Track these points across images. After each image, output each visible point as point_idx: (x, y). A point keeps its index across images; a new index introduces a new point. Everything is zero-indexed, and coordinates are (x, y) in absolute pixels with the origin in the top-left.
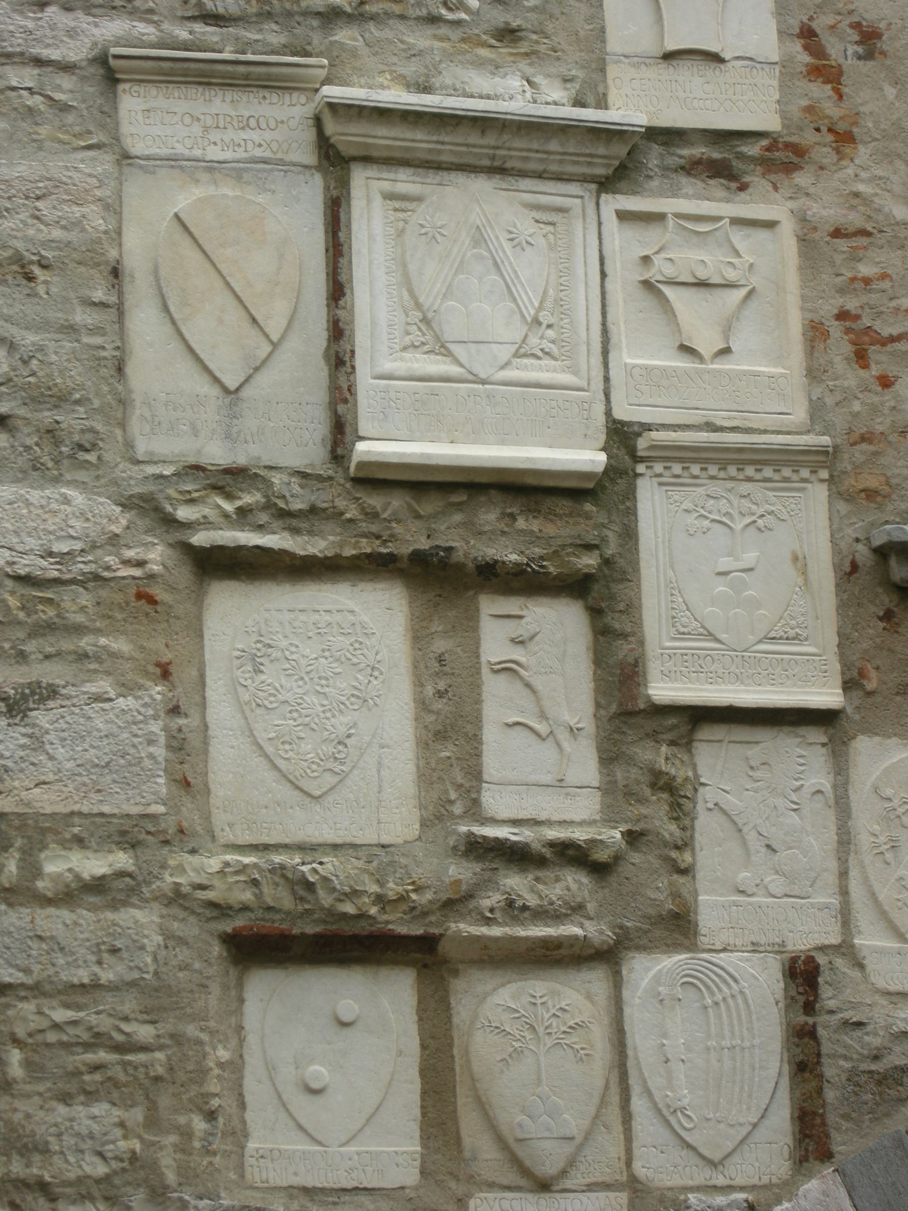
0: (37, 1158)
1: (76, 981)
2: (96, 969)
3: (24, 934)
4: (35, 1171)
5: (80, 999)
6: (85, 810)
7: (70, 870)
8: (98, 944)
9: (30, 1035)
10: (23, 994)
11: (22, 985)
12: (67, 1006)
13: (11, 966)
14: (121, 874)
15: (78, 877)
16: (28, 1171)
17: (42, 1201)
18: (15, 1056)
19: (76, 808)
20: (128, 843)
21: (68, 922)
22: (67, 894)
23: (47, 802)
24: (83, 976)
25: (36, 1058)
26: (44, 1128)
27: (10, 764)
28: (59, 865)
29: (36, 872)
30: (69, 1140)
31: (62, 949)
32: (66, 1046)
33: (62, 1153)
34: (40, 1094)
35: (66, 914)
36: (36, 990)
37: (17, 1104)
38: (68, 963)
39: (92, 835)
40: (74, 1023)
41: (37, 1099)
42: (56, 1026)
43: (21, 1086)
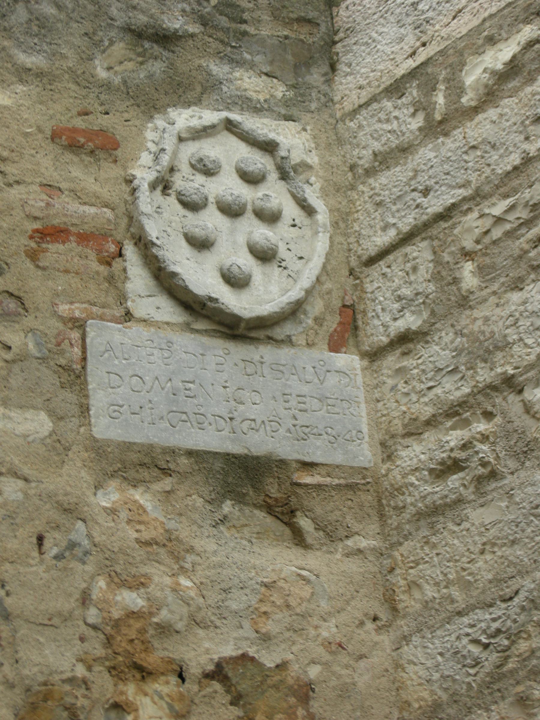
0: (499, 355)
1: (509, 168)
2: (526, 146)
3: (459, 152)
4: (499, 370)
5: (515, 183)
6: (494, 10)
7: (485, 71)
8: (523, 122)
9: (478, 242)
10: (465, 207)
11: (465, 199)
12: (506, 196)
13: (453, 187)
14: (530, 44)
15: (494, 73)
16: (493, 374)
17: (512, 398)
18: (469, 267)
19: (486, 14)
20: (533, 14)
21: (494, 118)
22: (488, 94)
23: (463, 26)
24: (515, 159)
25: (487, 260)
26: (501, 323)
27: (430, 14)
28: (475, 75)
29: (461, 90)
30: (524, 323)
31: (493, 146)
32: (508, 234)
33: (521, 339)
34: (494, 293)
35: (492, 113)
36: (478, 197)
37: (476, 313)
38: (501, 156)
39: (501, 27)
40: (512, 208)
41: (493, 299)
42: (499, 220)
43: (478, 294)
